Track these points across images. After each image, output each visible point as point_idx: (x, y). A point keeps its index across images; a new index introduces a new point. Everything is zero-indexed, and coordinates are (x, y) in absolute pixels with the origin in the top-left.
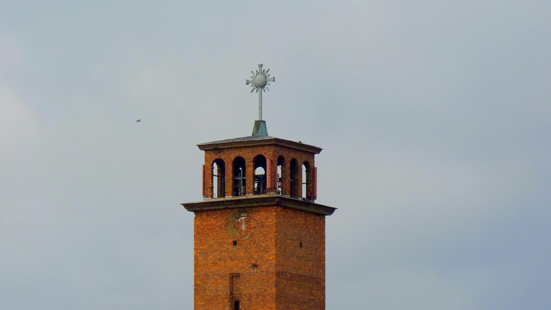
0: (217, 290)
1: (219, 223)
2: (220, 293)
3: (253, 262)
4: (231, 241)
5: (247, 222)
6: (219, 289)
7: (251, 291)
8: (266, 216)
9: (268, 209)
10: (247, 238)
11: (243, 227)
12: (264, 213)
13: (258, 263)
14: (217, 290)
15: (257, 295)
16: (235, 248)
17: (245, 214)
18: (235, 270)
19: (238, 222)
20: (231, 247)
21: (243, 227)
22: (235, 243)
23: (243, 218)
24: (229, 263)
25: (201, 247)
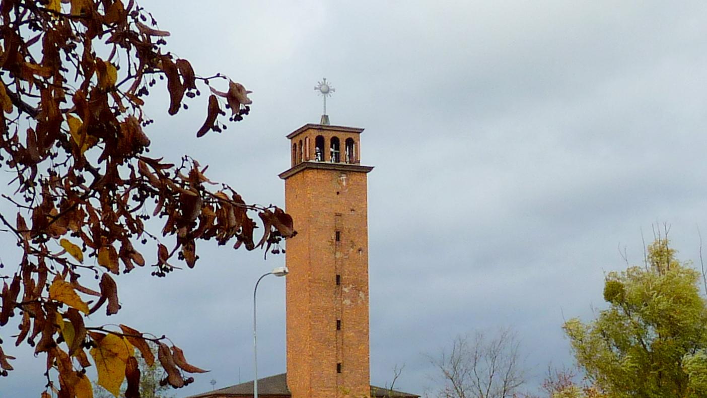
0: (325, 223)
1: (326, 178)
2: (328, 225)
3: (351, 207)
4: (335, 191)
5: (347, 180)
6: (326, 222)
7: (350, 227)
8: (360, 178)
9: (362, 174)
10: (347, 190)
11: (344, 183)
12: (359, 177)
13: (355, 209)
14: (325, 223)
15: (355, 230)
16: (339, 196)
17: (345, 175)
18: (339, 211)
19: (340, 180)
20: (335, 195)
21: (344, 183)
22: (338, 193)
23: (344, 178)
24: (334, 206)
25: (314, 193)
